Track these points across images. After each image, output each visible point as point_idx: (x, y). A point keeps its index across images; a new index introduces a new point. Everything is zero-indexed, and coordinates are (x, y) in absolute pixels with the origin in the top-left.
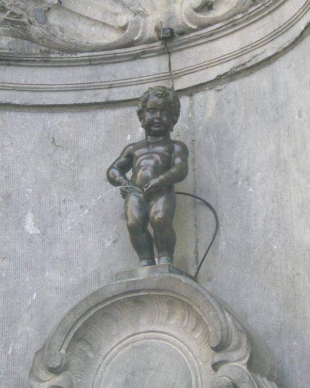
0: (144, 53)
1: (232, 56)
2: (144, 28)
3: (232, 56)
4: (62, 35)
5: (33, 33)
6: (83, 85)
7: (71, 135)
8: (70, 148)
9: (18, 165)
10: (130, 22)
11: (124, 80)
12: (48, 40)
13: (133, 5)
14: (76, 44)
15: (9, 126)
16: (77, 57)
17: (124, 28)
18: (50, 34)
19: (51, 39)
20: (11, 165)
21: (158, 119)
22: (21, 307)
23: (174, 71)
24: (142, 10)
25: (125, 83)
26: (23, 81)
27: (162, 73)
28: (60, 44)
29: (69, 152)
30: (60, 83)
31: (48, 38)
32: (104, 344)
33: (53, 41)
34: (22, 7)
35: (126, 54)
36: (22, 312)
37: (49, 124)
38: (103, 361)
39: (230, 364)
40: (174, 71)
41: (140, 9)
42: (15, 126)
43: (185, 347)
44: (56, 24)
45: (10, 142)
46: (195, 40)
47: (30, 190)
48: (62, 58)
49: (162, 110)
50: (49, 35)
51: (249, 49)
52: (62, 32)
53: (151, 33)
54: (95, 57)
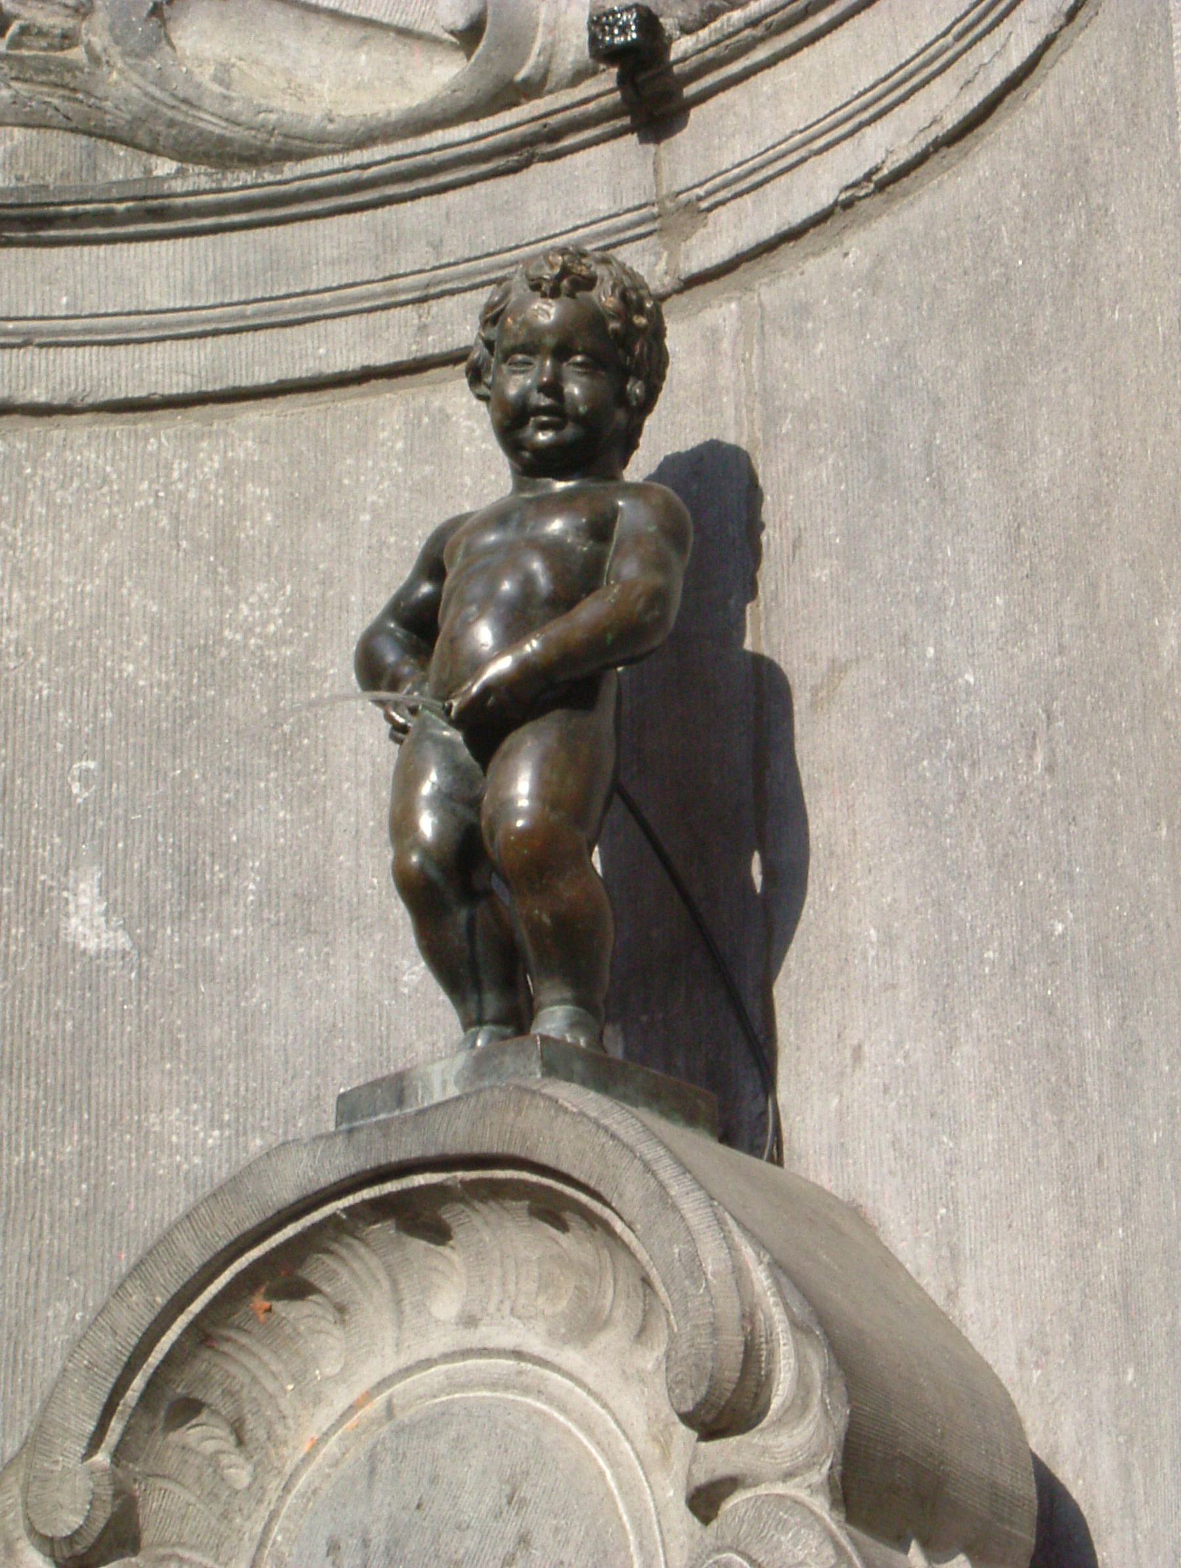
4: (225, 97)
5: (106, 99)
7: (269, 518)
8: (263, 571)
9: (43, 660)
11: (477, 258)
12: (172, 123)
16: (280, 183)
17: (470, 36)
18: (173, 96)
19: (180, 117)
20: (12, 665)
21: (544, 389)
22: (38, 1273)
27: (629, 211)
30: (218, 301)
32: (290, 1422)
33: (191, 127)
35: (481, 145)
37: (176, 475)
38: (281, 1499)
39: (762, 1490)
42: (32, 497)
43: (609, 1417)
45: (9, 565)
47: (92, 765)
48: (220, 191)
49: (561, 353)
51: (947, 48)
52: (221, 82)
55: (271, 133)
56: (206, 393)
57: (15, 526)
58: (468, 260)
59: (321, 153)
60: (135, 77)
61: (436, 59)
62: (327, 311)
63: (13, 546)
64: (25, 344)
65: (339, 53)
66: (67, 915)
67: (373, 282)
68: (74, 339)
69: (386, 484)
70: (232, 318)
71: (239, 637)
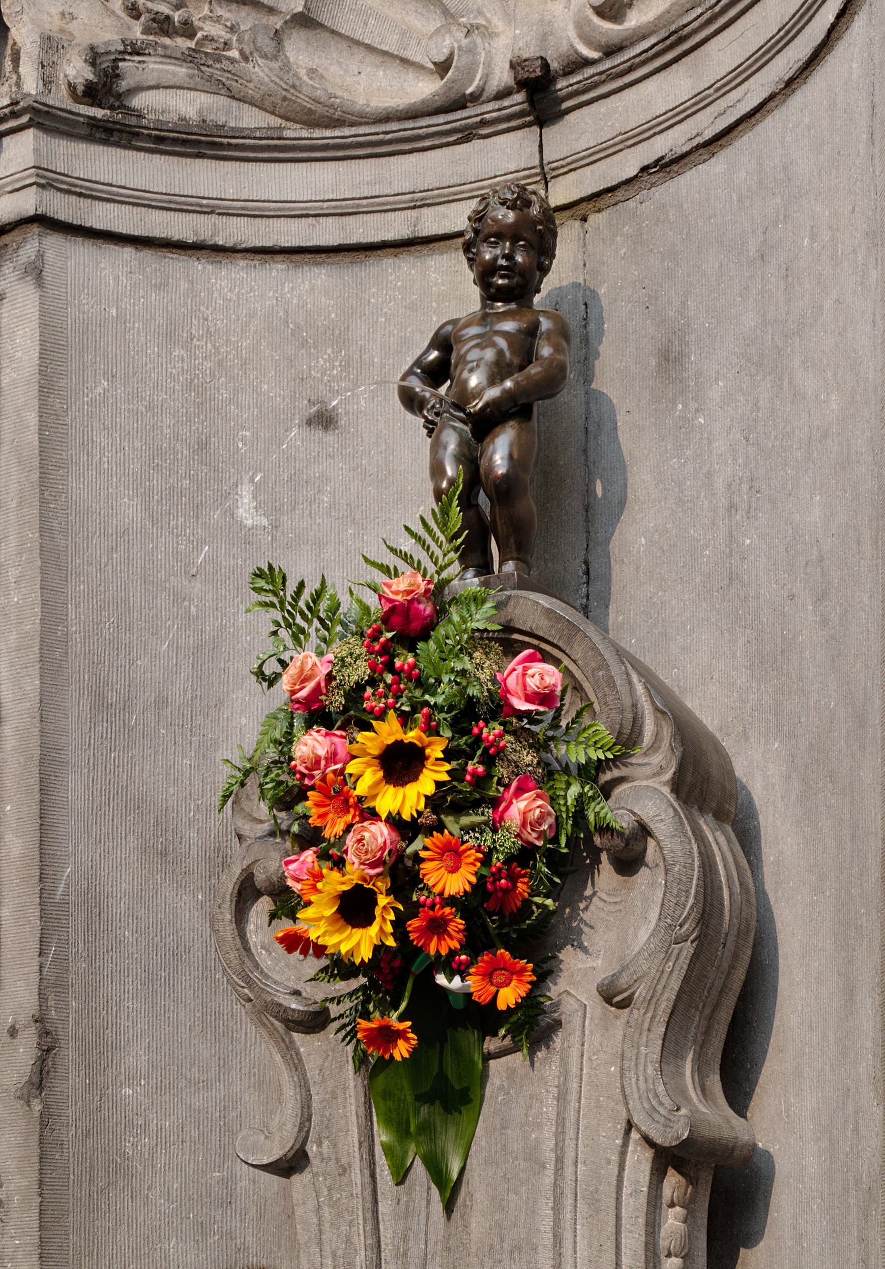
0: (484, 123)
1: (675, 116)
2: (488, 65)
3: (675, 116)
5: (250, 81)
6: (356, 202)
8: (331, 343)
9: (223, 379)
10: (456, 51)
11: (443, 188)
12: (285, 99)
13: (464, 13)
14: (344, 109)
15: (202, 294)
17: (443, 67)
19: (289, 96)
20: (208, 380)
23: (549, 163)
24: (484, 23)
25: (445, 196)
26: (230, 193)
27: (525, 170)
28: (310, 109)
29: (329, 351)
30: (309, 198)
31: (284, 93)
33: (295, 102)
34: (229, 24)
36: (231, 688)
37: (286, 290)
40: (549, 163)
41: (481, 21)
44: (301, 62)
46: (596, 85)
47: (248, 434)
50: (284, 86)
53: (502, 76)
54: (381, 136)
55: (336, 110)
56: (302, 247)
57: (207, 309)
58: (438, 189)
59: (360, 124)
60: (266, 70)
61: (421, 78)
62: (365, 209)
63: (206, 320)
64: (212, 212)
65: (369, 69)
66: (237, 507)
67: (389, 196)
68: (236, 212)
69: (392, 303)
70: (316, 208)
71: (319, 375)
